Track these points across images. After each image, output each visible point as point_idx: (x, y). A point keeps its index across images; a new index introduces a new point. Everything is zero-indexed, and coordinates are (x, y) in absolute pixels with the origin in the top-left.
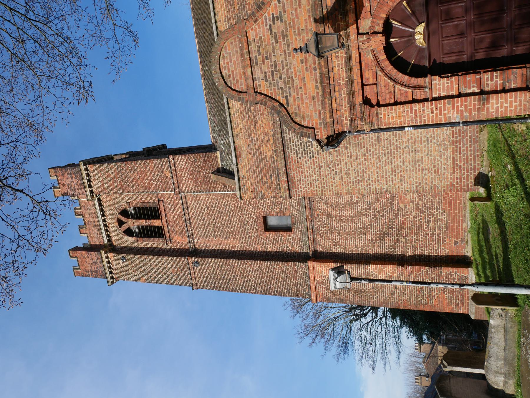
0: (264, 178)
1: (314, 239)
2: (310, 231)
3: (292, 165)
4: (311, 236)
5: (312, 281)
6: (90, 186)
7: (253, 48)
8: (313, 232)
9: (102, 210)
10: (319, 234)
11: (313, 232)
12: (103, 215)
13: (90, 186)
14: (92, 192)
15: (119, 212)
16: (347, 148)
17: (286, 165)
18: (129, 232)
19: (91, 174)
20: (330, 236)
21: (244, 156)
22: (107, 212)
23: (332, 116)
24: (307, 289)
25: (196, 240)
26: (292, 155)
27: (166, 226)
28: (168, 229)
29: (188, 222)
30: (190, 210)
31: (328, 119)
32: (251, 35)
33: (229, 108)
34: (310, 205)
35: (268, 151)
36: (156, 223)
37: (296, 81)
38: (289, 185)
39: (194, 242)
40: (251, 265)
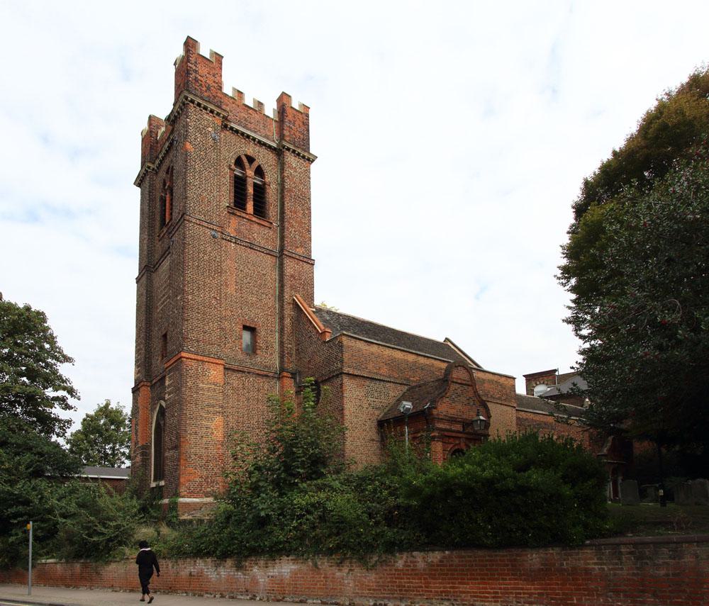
0: (355, 358)
1: (238, 371)
2: (246, 370)
3: (362, 381)
4: (240, 368)
5: (205, 359)
6: (294, 151)
7: (466, 387)
8: (244, 372)
9: (265, 144)
10: (242, 377)
11: (244, 372)
12: (259, 142)
13: (294, 151)
14: (288, 149)
15: (262, 166)
16: (370, 419)
17: (362, 376)
18: (239, 162)
19: (302, 161)
20: (241, 386)
21: (367, 348)
22: (263, 150)
23: (441, 419)
24: (193, 350)
25: (233, 245)
26: (368, 383)
27: (244, 215)
28: (243, 218)
29: (251, 246)
30: (263, 254)
31: (440, 417)
32: (470, 388)
33: (393, 348)
34: (267, 376)
35: (370, 366)
36: (250, 207)
37: (454, 404)
38: (350, 374)
39: (231, 242)
40: (216, 298)
